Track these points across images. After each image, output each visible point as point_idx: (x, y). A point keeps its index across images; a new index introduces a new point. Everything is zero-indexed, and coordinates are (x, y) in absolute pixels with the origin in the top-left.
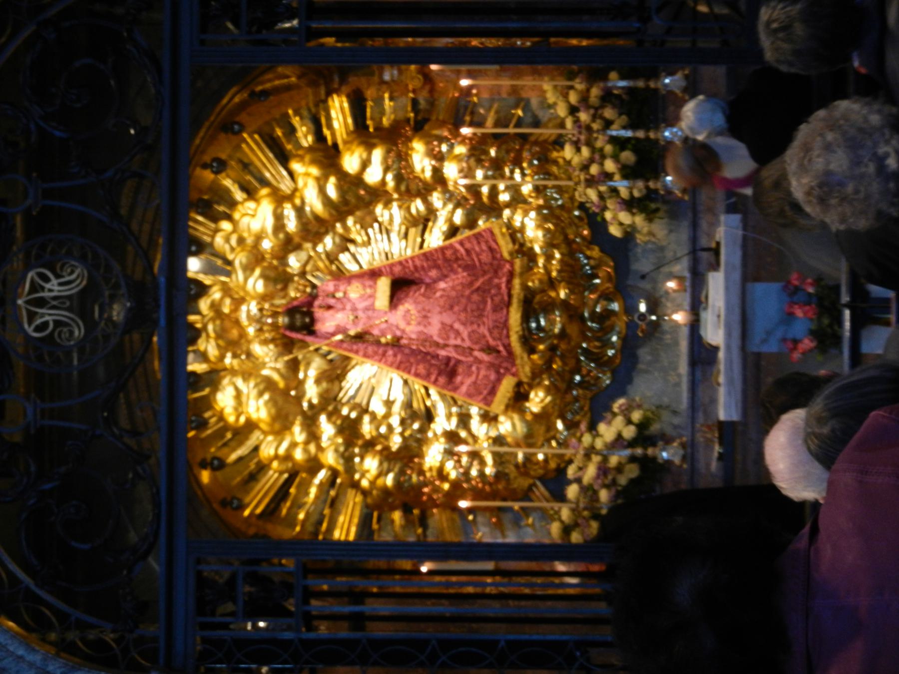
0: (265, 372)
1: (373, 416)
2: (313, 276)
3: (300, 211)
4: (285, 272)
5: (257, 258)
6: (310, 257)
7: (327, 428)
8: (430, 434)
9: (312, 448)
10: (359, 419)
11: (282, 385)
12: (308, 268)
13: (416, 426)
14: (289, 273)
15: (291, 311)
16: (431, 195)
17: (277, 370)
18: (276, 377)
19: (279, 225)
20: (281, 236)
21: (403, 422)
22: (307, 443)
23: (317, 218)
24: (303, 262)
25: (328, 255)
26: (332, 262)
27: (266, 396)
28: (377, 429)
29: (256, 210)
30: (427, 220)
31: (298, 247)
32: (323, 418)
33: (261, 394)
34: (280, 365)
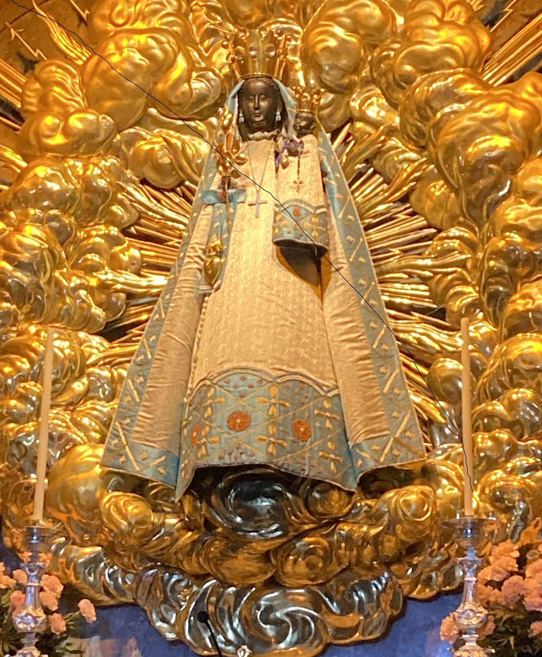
1: (113, 241)
2: (348, 135)
3: (449, 95)
5: (372, 36)
6: (375, 125)
7: (99, 170)
8: (82, 335)
9: (59, 140)
10: (113, 221)
11: (160, 86)
12: (359, 125)
13: (97, 311)
16: (485, 319)
19: (428, 64)
20: (408, 68)
21: (104, 286)
22: (66, 132)
23: (437, 127)
27: (137, 57)
28: (94, 250)
29: (453, 24)
30: (441, 314)
31: (393, 105)
32: (112, 161)
33: (144, 51)
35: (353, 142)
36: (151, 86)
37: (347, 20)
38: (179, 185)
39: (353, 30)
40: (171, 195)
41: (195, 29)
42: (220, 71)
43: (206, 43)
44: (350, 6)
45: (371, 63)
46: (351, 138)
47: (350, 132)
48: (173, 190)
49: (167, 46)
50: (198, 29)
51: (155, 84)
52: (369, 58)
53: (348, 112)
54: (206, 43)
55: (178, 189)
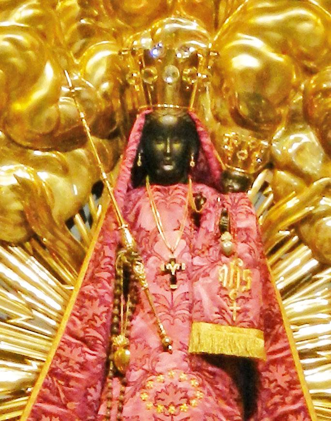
0: (49, 72)
2: (265, 185)
4: (275, 122)
6: (307, 179)
11: (19, 107)
12: (282, 175)
14: (273, 131)
15: (188, 130)
17: (52, 99)
18: (38, 94)
24: (298, 162)
25: (309, 219)
26: (295, 227)
34: (67, 106)
35: (271, 196)
36: (4, 103)
37: (276, 36)
38: (29, 240)
39: (282, 48)
40: (17, 250)
41: (62, 24)
42: (98, 87)
43: (77, 46)
44: (280, 17)
45: (304, 93)
46: (270, 189)
47: (269, 181)
48: (20, 244)
49: (30, 53)
50: (69, 24)
51: (9, 100)
52: (303, 86)
53: (268, 155)
54: (77, 46)
55: (28, 244)
